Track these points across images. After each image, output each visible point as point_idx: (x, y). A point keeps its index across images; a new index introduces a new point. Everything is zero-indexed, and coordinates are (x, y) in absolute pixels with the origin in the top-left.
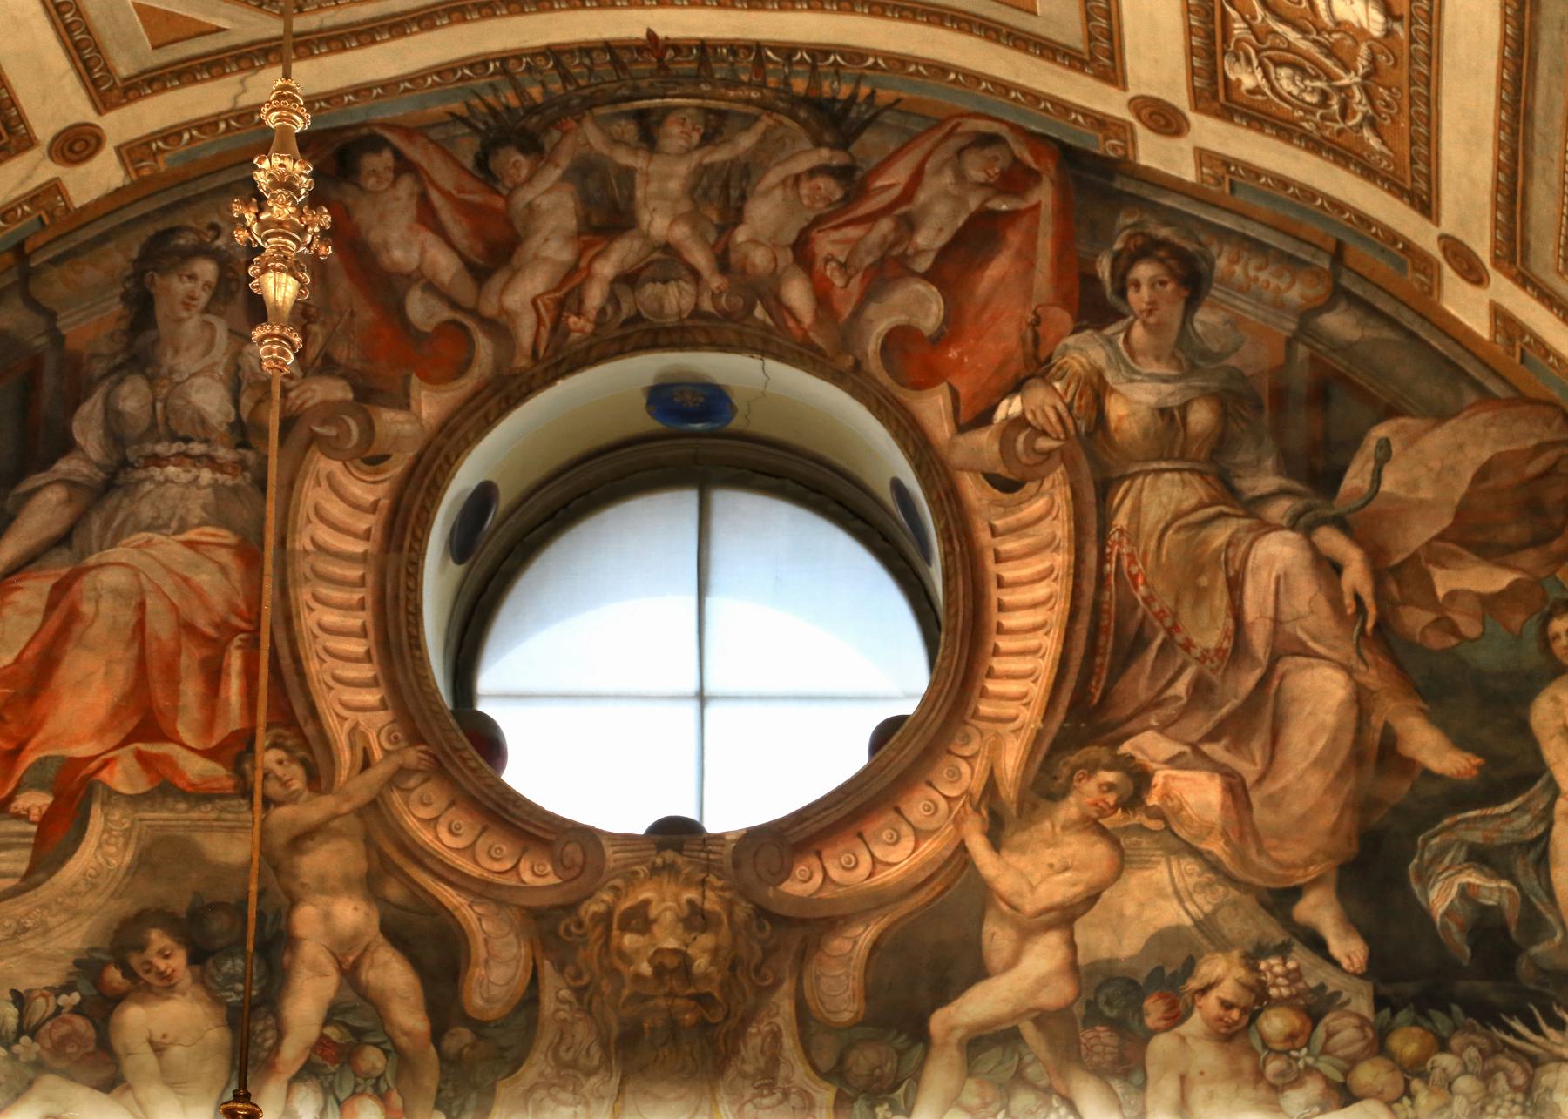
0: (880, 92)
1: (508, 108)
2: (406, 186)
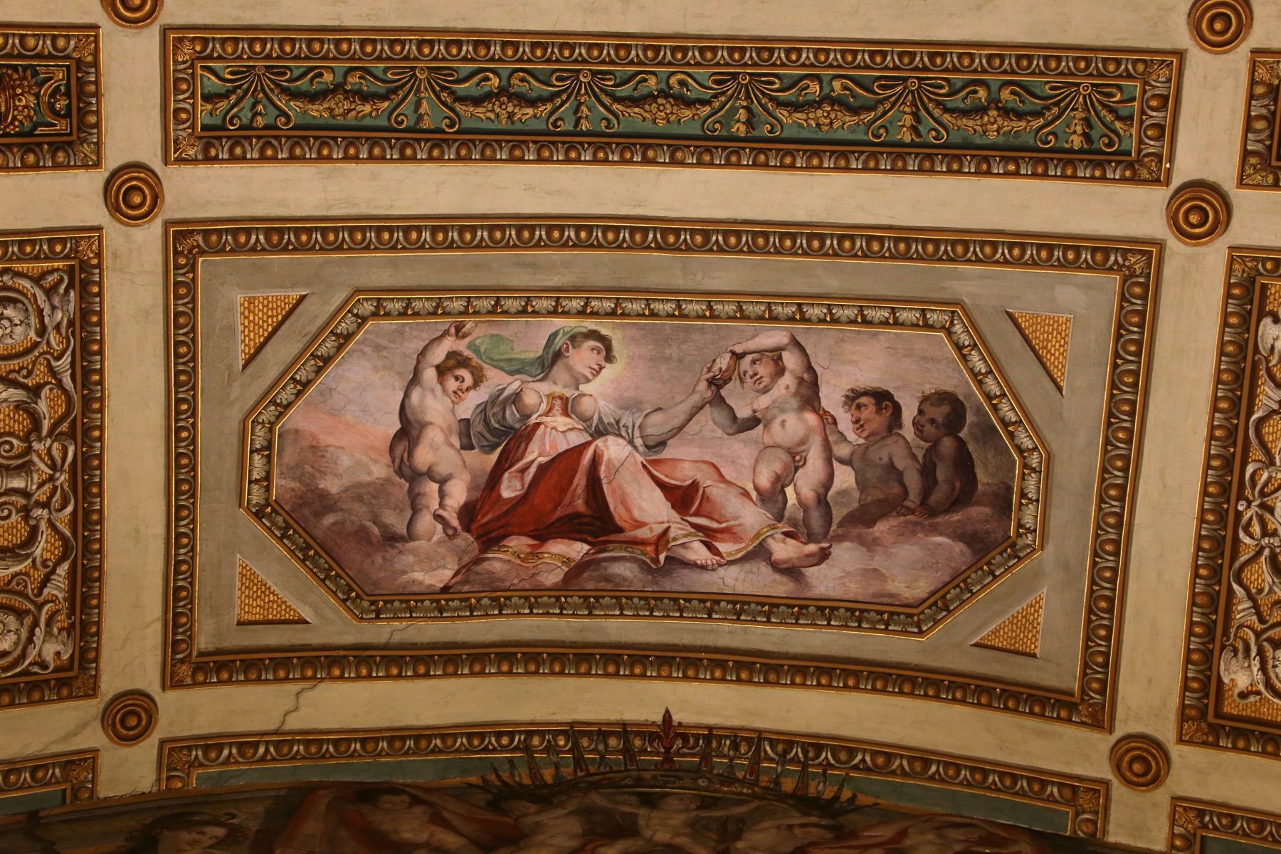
0: (860, 797)
1: (520, 784)
2: (418, 810)
